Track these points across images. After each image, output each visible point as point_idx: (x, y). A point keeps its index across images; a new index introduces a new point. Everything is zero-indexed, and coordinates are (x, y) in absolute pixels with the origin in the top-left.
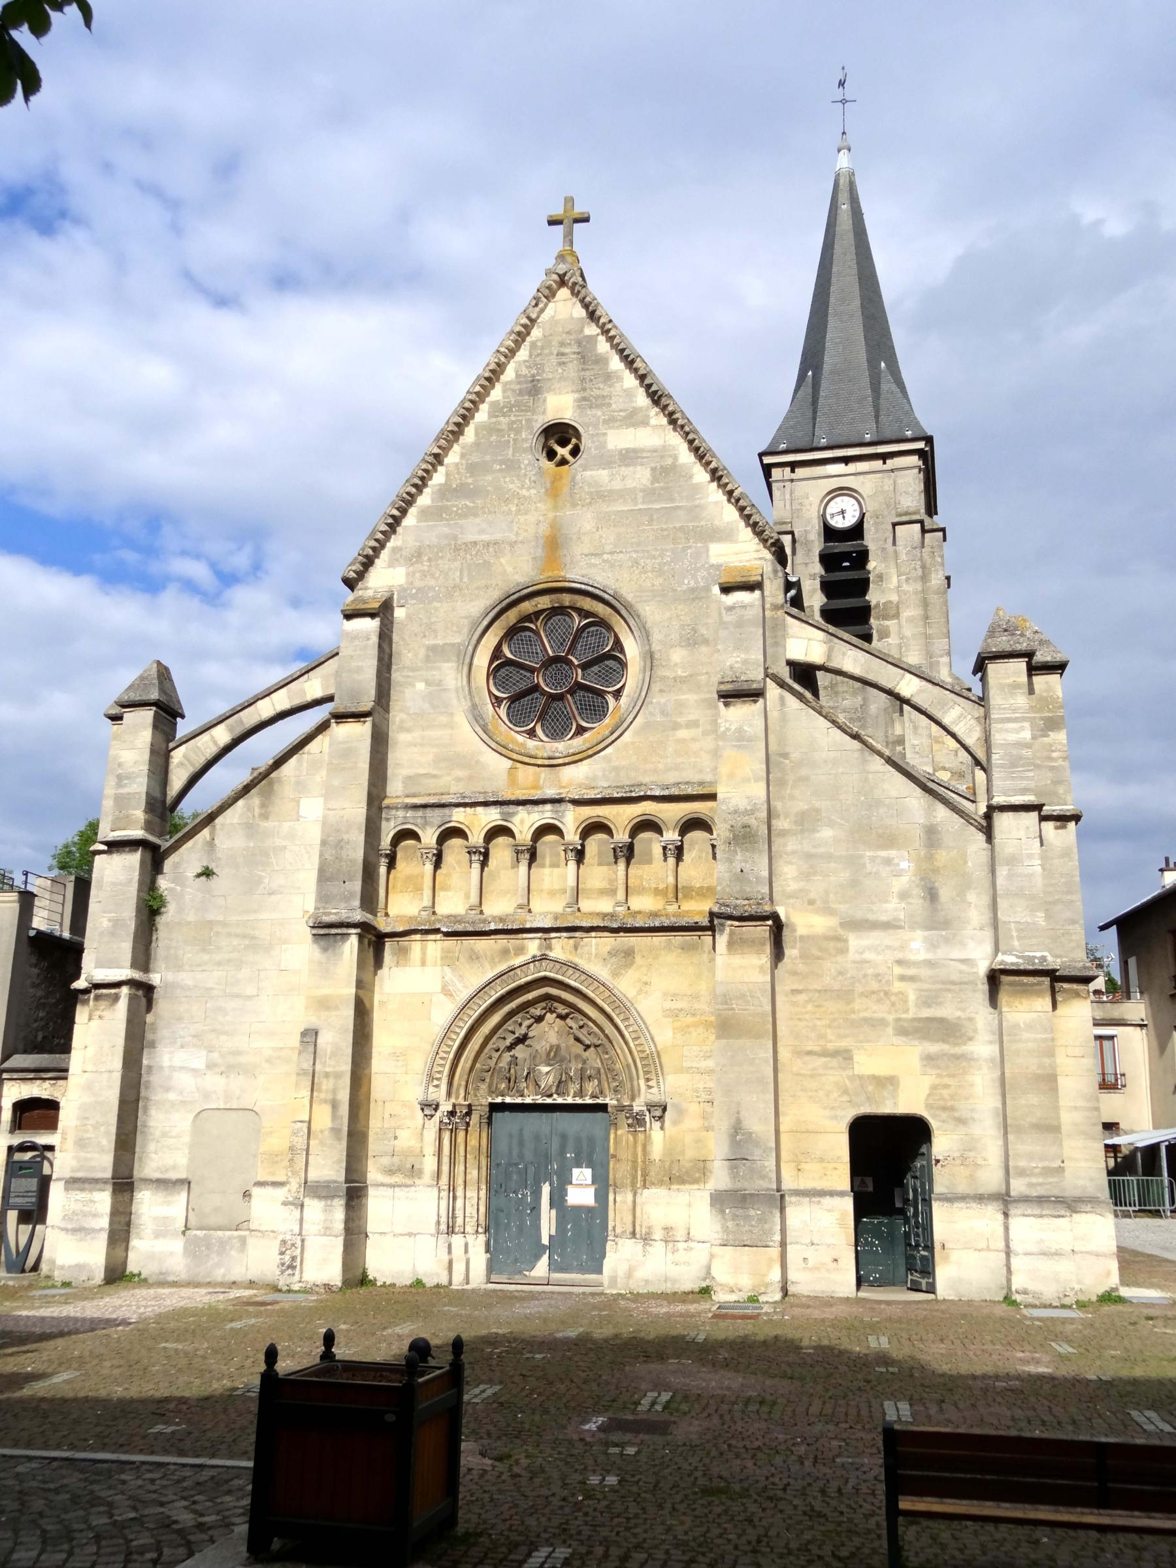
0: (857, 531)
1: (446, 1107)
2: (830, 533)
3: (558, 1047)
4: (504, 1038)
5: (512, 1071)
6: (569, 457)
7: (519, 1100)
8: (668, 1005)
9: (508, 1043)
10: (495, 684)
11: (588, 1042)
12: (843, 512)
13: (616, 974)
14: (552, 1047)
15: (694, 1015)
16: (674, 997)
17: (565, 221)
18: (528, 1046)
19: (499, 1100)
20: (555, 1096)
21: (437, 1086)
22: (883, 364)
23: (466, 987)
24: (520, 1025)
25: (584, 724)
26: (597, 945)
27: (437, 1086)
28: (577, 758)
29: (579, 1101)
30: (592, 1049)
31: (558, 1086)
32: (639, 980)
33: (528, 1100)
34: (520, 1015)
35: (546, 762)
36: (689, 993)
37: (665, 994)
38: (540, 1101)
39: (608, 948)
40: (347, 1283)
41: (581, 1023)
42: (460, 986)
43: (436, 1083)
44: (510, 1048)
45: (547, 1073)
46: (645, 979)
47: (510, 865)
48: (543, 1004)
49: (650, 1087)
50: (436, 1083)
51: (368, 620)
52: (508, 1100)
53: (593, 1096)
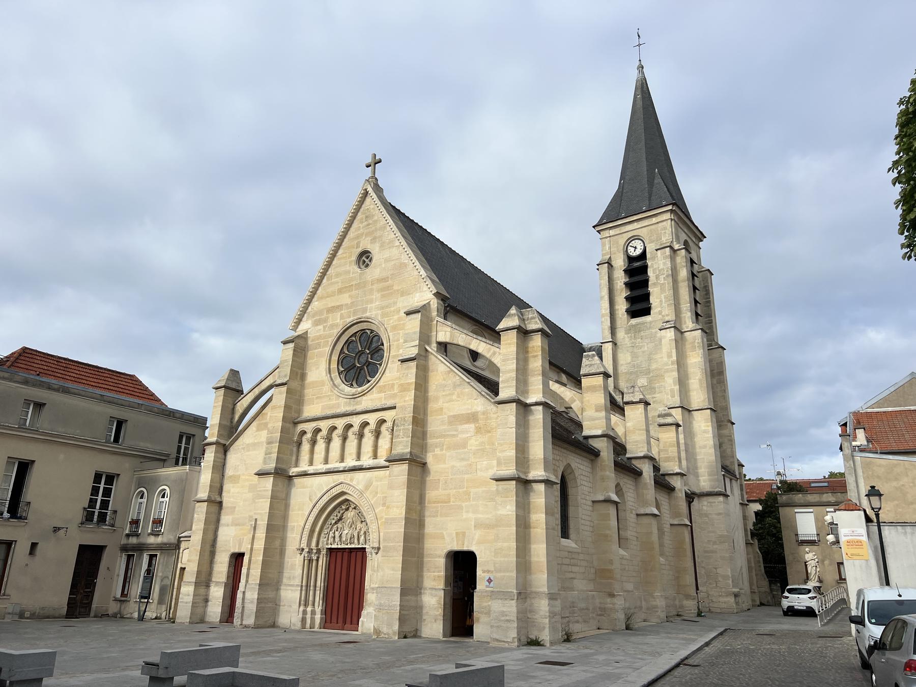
0: (643, 256)
1: (306, 550)
2: (631, 259)
4: (333, 519)
6: (369, 263)
9: (334, 522)
10: (342, 365)
12: (636, 248)
17: (372, 164)
22: (656, 170)
24: (339, 512)
25: (369, 379)
28: (364, 394)
29: (357, 546)
34: (338, 509)
35: (351, 397)
40: (257, 627)
44: (336, 523)
48: (346, 503)
51: (291, 344)
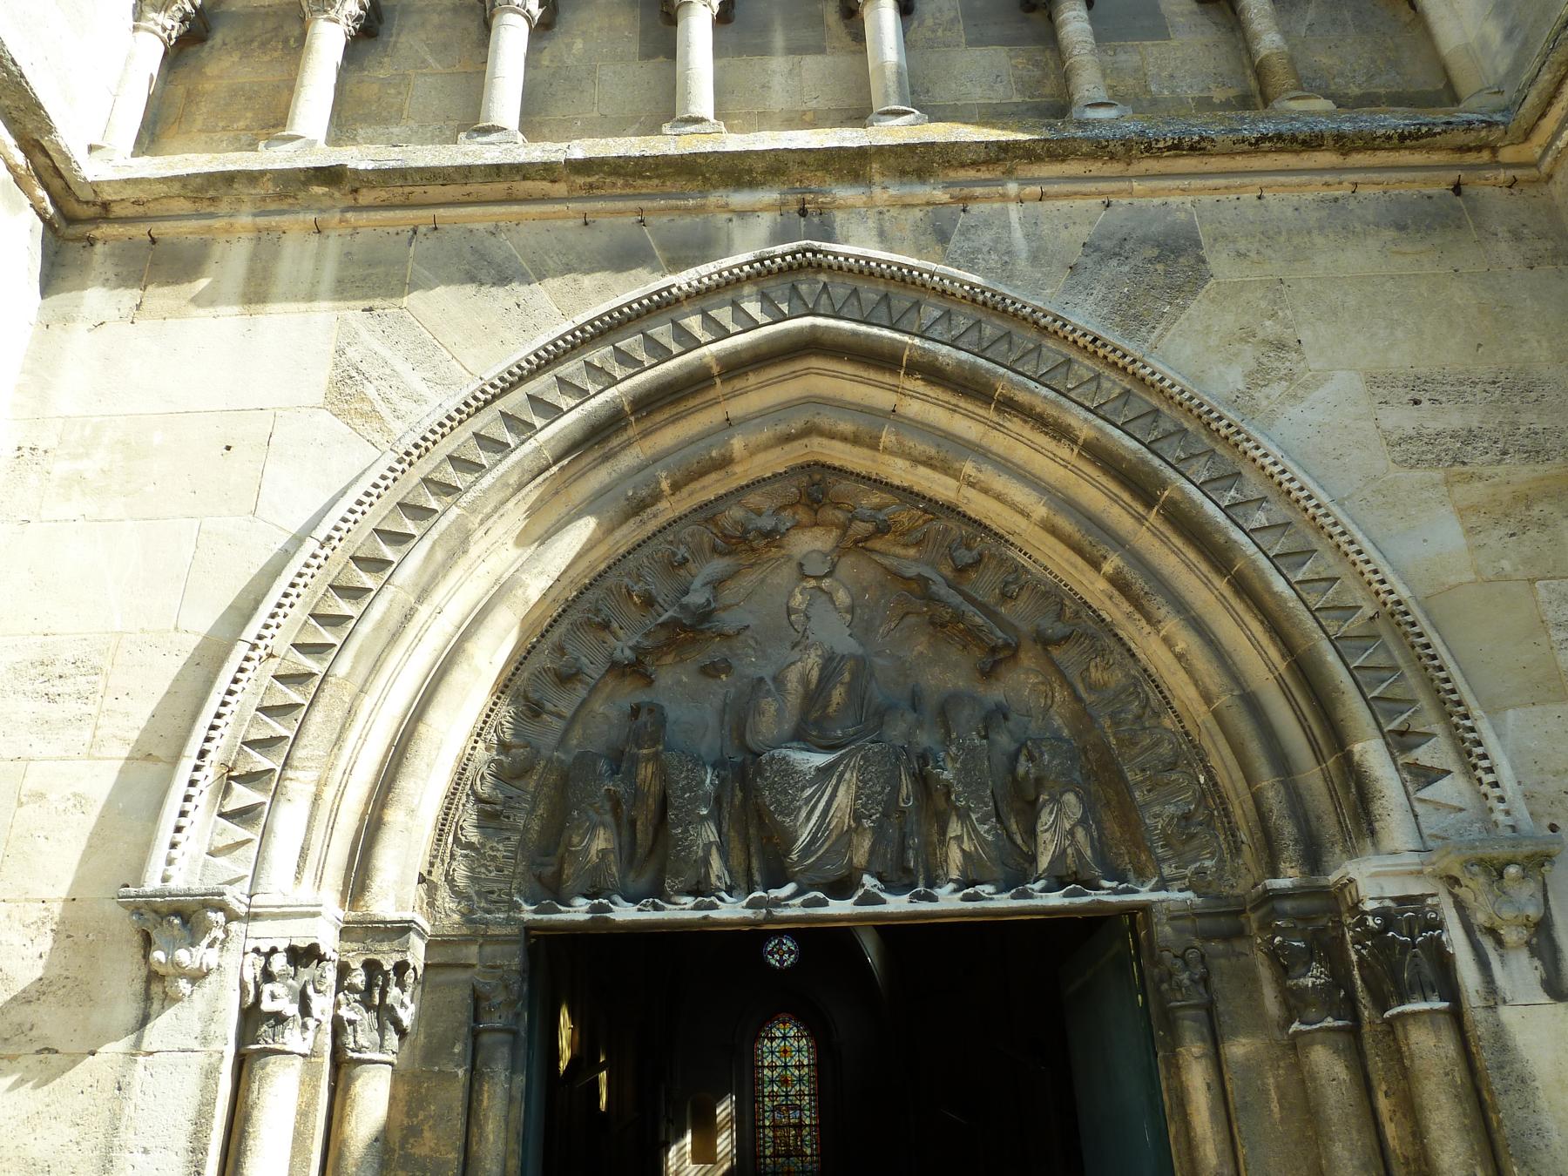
3: (861, 667)
5: (646, 772)
7: (683, 910)
8: (1401, 419)
9: (623, 646)
11: (999, 636)
13: (1132, 317)
14: (831, 665)
15: (1535, 453)
16: (1419, 390)
18: (710, 671)
19: (579, 911)
20: (869, 881)
21: (243, 815)
23: (442, 382)
26: (1032, 225)
27: (243, 815)
30: (1028, 658)
31: (879, 832)
32: (1248, 335)
33: (731, 910)
36: (1483, 371)
37: (1373, 381)
38: (795, 910)
39: (1084, 232)
41: (966, 557)
42: (415, 381)
43: (242, 796)
44: (636, 669)
45: (824, 772)
46: (1270, 328)
47: (635, 48)
49: (1427, 775)
50: (242, 796)
52: (624, 913)
53: (1057, 882)
